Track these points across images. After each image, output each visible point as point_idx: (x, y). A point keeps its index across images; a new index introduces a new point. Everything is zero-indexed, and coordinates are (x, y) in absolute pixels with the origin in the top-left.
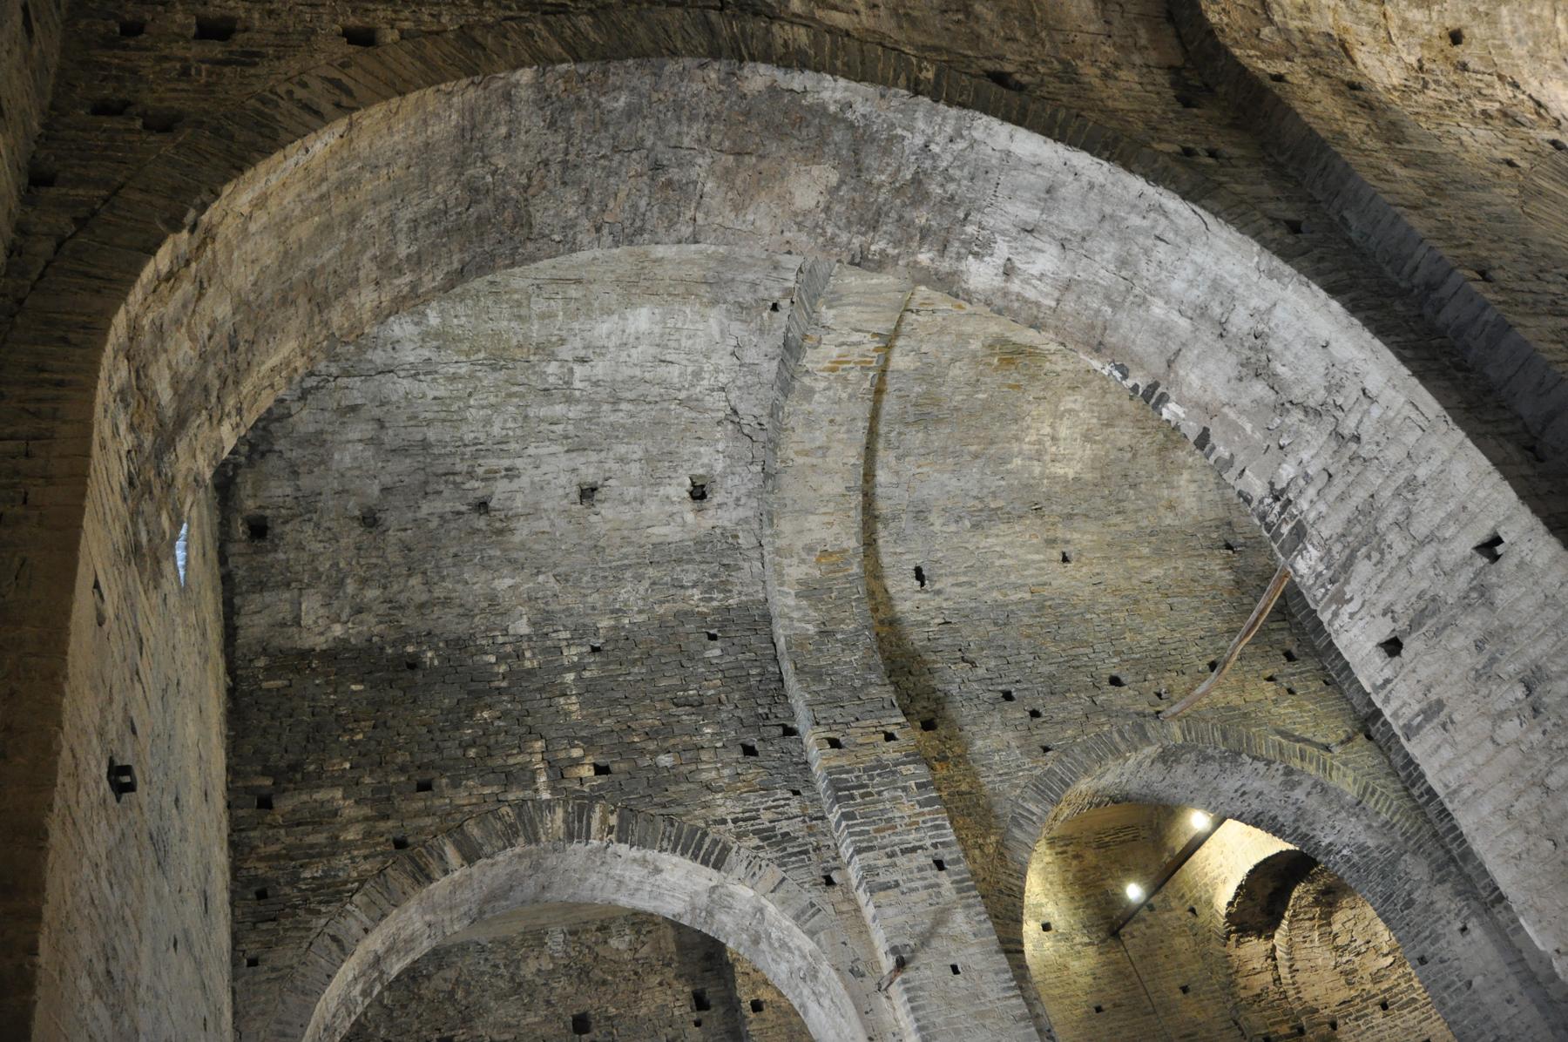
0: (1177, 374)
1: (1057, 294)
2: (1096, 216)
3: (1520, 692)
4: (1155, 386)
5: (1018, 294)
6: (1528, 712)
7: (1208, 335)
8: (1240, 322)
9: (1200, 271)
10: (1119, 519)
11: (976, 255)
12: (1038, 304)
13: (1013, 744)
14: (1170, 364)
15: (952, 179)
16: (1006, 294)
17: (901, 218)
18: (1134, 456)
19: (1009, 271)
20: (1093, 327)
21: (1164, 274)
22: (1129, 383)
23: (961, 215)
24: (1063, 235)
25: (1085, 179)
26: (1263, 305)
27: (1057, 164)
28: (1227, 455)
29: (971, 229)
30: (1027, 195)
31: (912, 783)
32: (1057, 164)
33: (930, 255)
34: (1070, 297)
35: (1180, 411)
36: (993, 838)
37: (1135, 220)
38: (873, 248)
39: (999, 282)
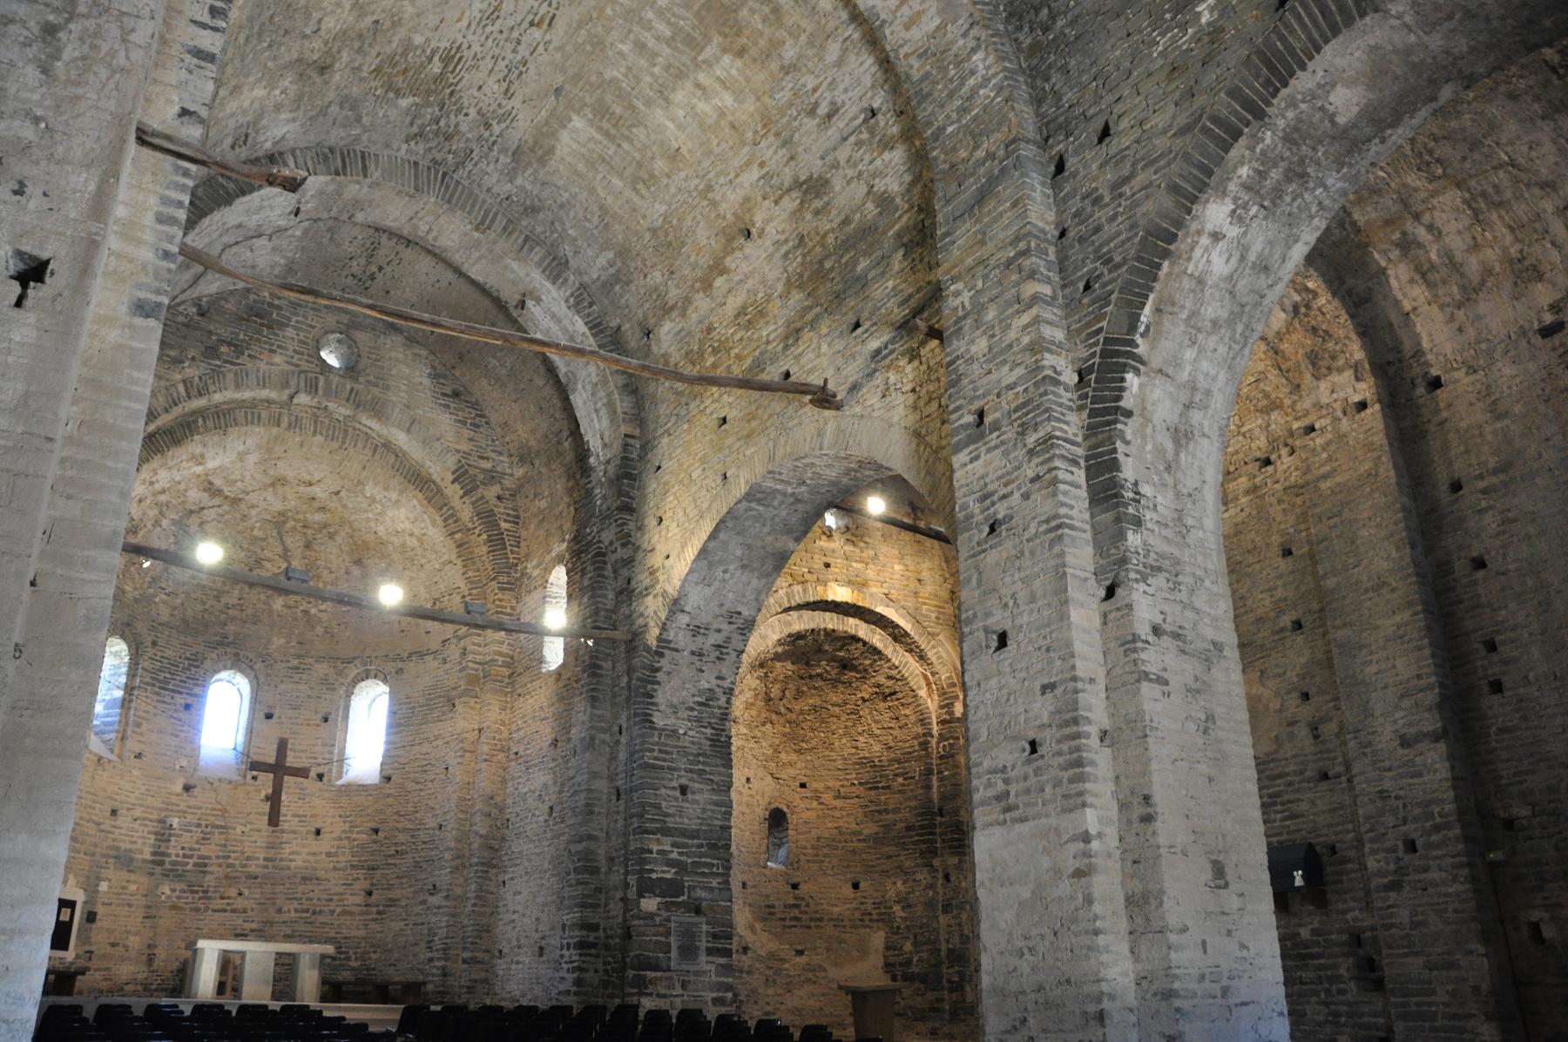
0: (1154, 378)
1: (1197, 274)
2: (1244, 300)
3: (1203, 717)
4: (1143, 363)
5: (1197, 243)
6: (1201, 729)
7: (1184, 396)
8: (1196, 416)
9: (1214, 379)
10: (242, 40)
11: (1234, 211)
12: (1189, 259)
14: (1160, 371)
15: (1294, 200)
16: (1199, 233)
17: (1283, 159)
18: (305, 37)
19: (1216, 237)
20: (1173, 304)
21: (1209, 354)
22: (1139, 340)
23: (1266, 204)
24: (1235, 277)
25: (1266, 292)
26: (1206, 430)
27: (1280, 274)
28: (1129, 437)
29: (1254, 210)
30: (1266, 252)
32: (1280, 274)
33: (1245, 176)
34: (1193, 284)
35: (1135, 389)
37: (1240, 328)
38: (1269, 133)
39: (1209, 227)
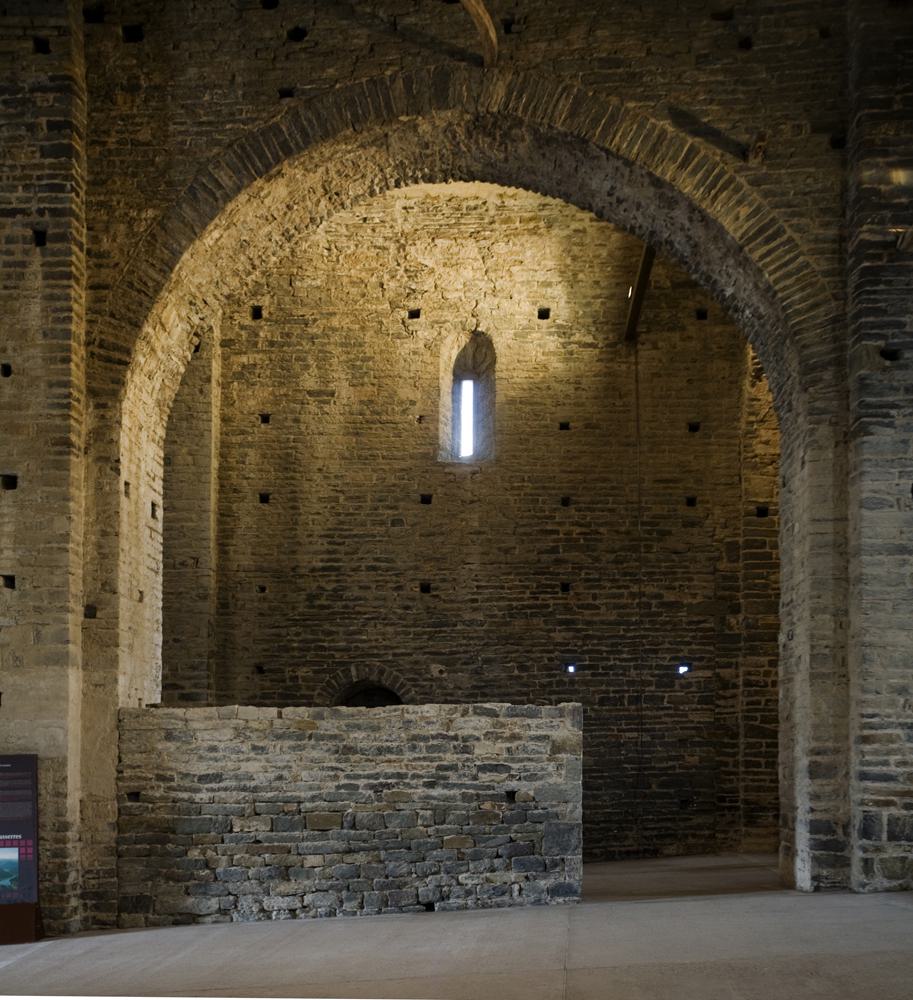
13: (239, 79)
31: (43, 120)
36: (151, 213)
